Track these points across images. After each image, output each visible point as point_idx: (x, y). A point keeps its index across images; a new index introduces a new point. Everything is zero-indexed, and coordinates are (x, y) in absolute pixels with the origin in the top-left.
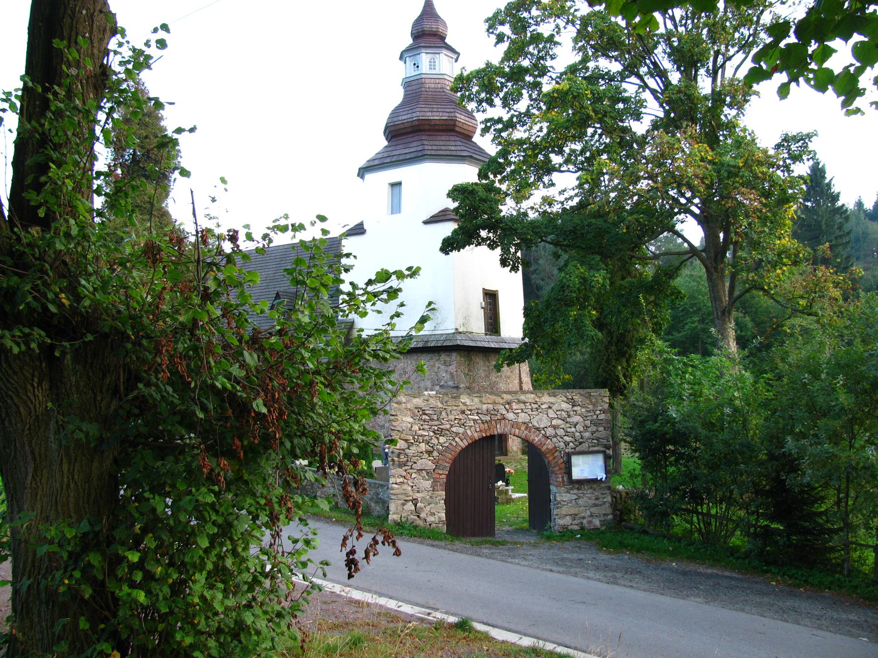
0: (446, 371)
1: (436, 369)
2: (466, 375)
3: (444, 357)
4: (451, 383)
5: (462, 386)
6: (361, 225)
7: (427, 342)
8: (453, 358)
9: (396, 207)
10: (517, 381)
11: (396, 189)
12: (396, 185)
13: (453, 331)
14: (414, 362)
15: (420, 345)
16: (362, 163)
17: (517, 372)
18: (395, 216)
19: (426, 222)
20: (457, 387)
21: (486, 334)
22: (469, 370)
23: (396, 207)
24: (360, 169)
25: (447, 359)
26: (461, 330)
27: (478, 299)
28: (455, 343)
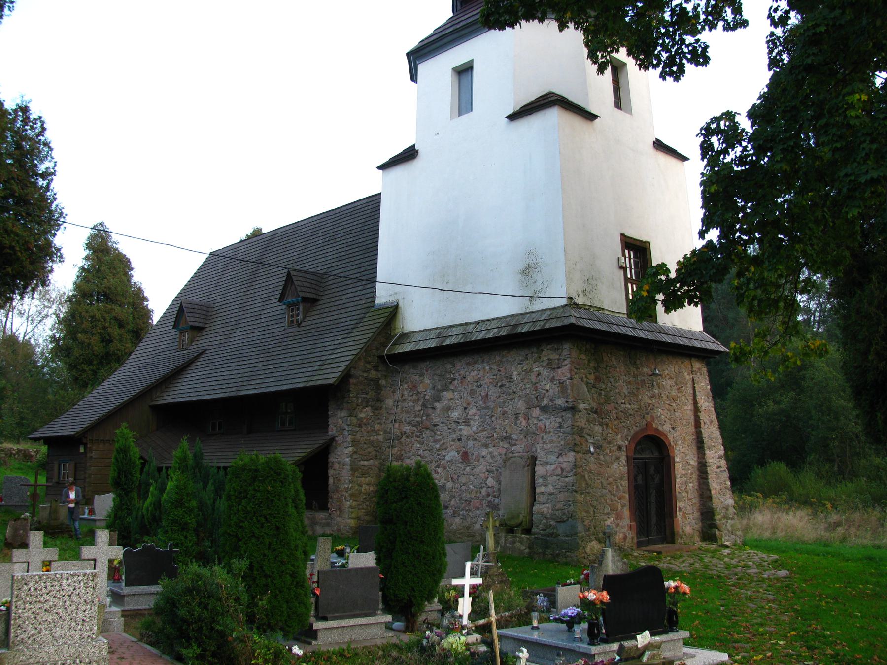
0: (553, 380)
1: (533, 378)
2: (591, 387)
3: (548, 353)
4: (560, 402)
5: (582, 406)
6: (414, 146)
7: (516, 325)
8: (565, 353)
9: (464, 103)
10: (689, 407)
11: (465, 78)
12: (464, 71)
13: (564, 302)
14: (495, 367)
15: (503, 333)
16: (413, 43)
17: (690, 391)
18: (465, 117)
19: (512, 117)
20: (573, 409)
21: (629, 316)
22: (598, 379)
23: (464, 103)
24: (409, 55)
25: (554, 356)
26: (580, 301)
27: (612, 252)
28: (566, 322)
